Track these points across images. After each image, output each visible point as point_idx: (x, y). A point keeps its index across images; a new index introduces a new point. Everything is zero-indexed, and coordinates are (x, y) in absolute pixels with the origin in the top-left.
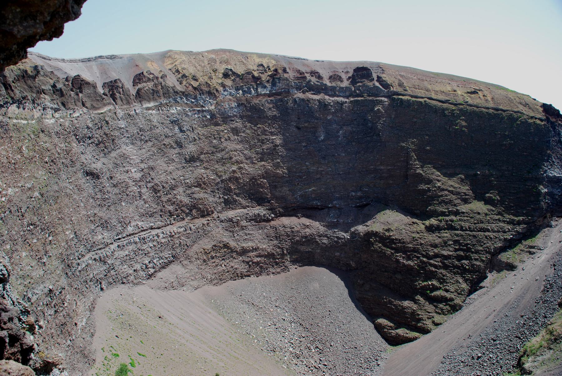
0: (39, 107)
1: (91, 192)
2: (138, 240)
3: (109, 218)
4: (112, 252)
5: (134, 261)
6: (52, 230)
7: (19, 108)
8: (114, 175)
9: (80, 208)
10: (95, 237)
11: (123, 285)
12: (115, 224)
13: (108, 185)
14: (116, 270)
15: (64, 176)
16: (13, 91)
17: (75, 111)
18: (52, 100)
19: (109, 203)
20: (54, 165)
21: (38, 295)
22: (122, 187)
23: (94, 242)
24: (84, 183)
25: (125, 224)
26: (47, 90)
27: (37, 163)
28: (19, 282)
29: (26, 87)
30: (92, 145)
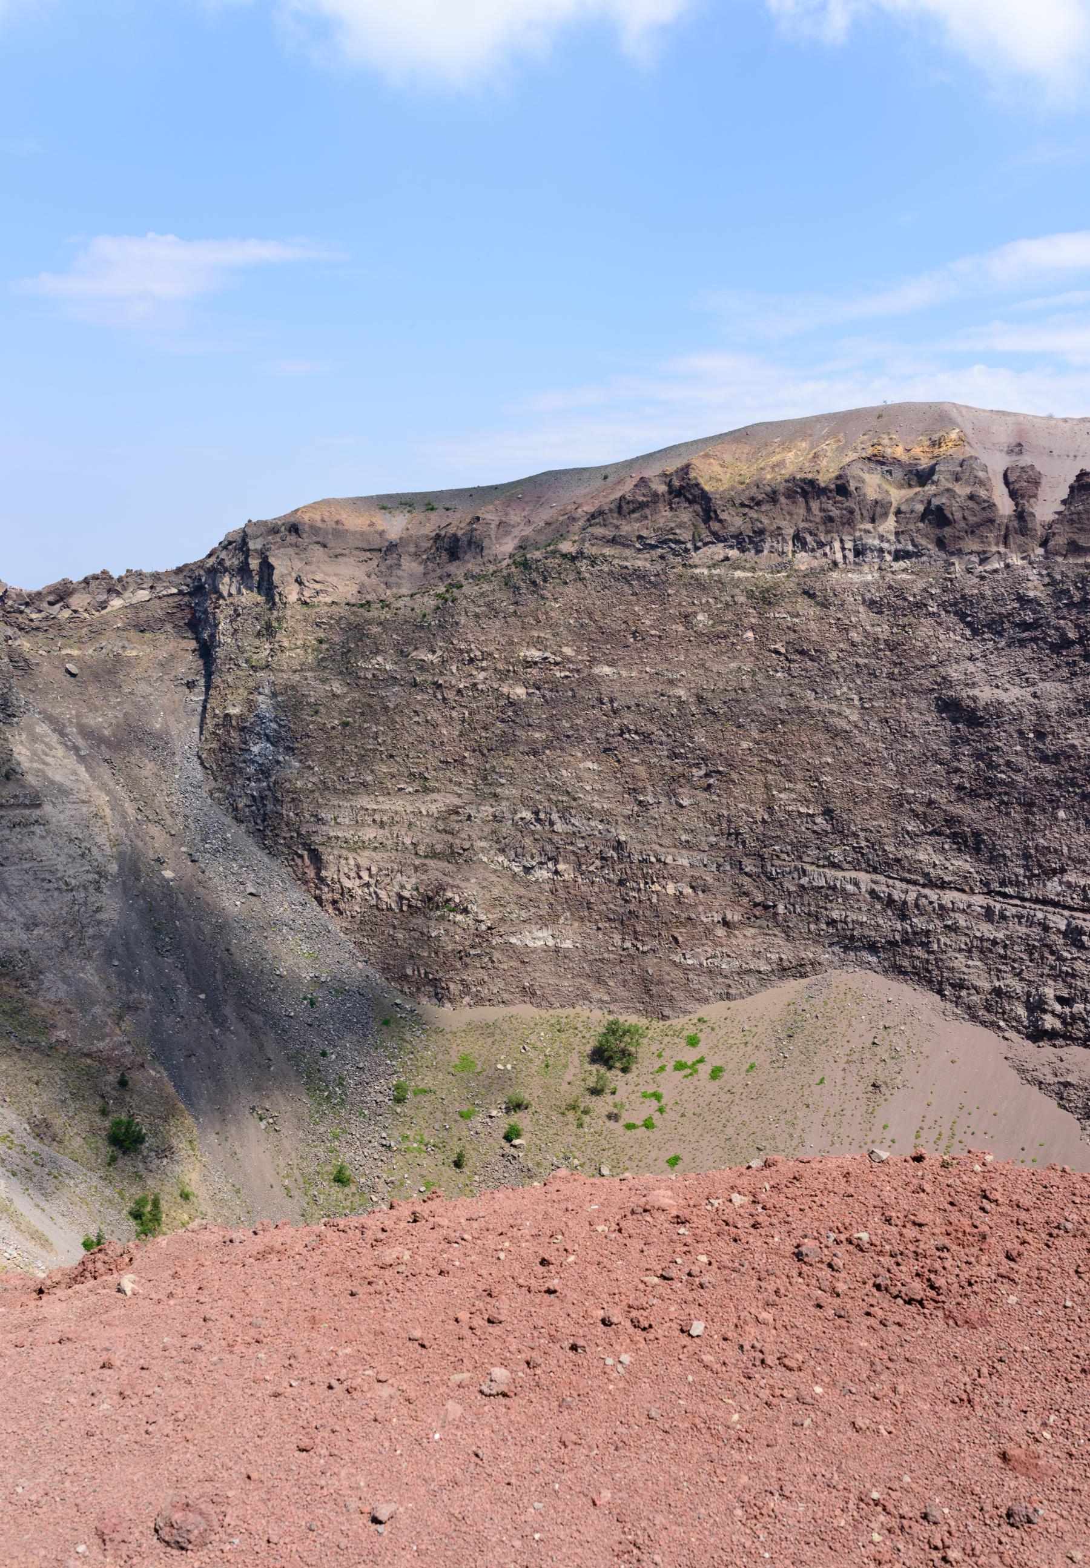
0: (827, 550)
1: (935, 747)
2: (1063, 928)
3: (989, 830)
4: (941, 907)
5: (1014, 968)
6: (721, 769)
7: (743, 550)
8: (1061, 730)
9: (876, 769)
10: (909, 852)
11: (938, 997)
12: (1008, 853)
13: (1018, 748)
14: (933, 952)
15: (845, 689)
16: (720, 521)
17: (987, 558)
18: (897, 534)
19: (1006, 794)
20: (809, 663)
21: (575, 829)
22: (1073, 770)
23: (898, 860)
24: (927, 723)
25: (1040, 866)
26: (905, 513)
27: (739, 648)
28: (538, 788)
29: (802, 511)
30: (1037, 645)
